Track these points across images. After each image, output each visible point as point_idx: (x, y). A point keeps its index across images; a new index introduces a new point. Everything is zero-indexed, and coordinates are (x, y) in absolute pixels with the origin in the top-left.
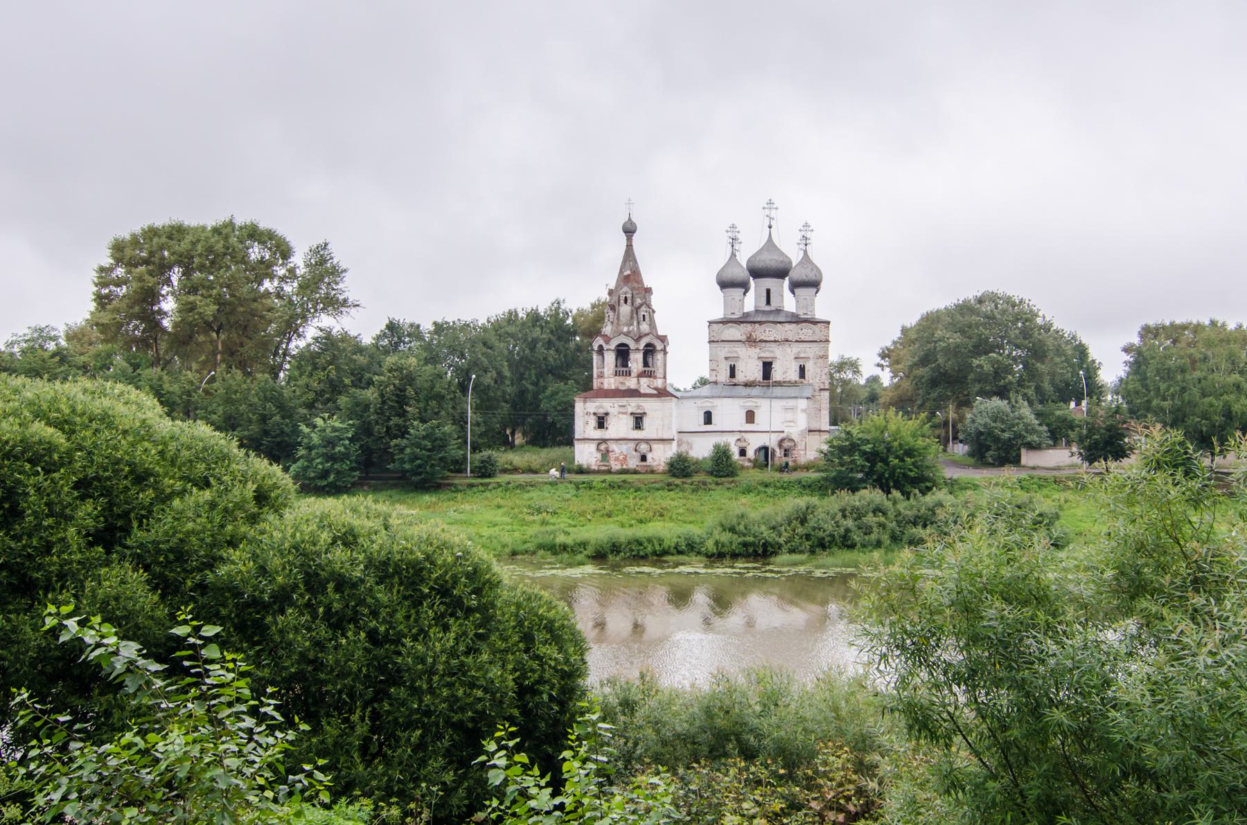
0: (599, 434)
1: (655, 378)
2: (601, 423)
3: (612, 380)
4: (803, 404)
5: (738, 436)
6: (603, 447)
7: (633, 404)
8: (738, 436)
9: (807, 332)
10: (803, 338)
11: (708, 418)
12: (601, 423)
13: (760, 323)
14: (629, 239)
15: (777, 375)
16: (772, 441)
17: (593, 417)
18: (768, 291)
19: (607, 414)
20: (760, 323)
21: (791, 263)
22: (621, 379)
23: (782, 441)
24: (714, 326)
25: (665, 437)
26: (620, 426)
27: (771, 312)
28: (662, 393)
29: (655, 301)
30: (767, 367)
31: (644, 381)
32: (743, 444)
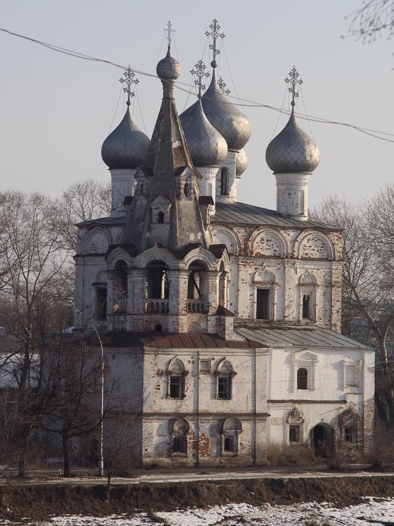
0: (170, 406)
2: (176, 389)
5: (290, 407)
8: (290, 407)
12: (176, 389)
16: (328, 415)
22: (195, 317)
30: (263, 297)
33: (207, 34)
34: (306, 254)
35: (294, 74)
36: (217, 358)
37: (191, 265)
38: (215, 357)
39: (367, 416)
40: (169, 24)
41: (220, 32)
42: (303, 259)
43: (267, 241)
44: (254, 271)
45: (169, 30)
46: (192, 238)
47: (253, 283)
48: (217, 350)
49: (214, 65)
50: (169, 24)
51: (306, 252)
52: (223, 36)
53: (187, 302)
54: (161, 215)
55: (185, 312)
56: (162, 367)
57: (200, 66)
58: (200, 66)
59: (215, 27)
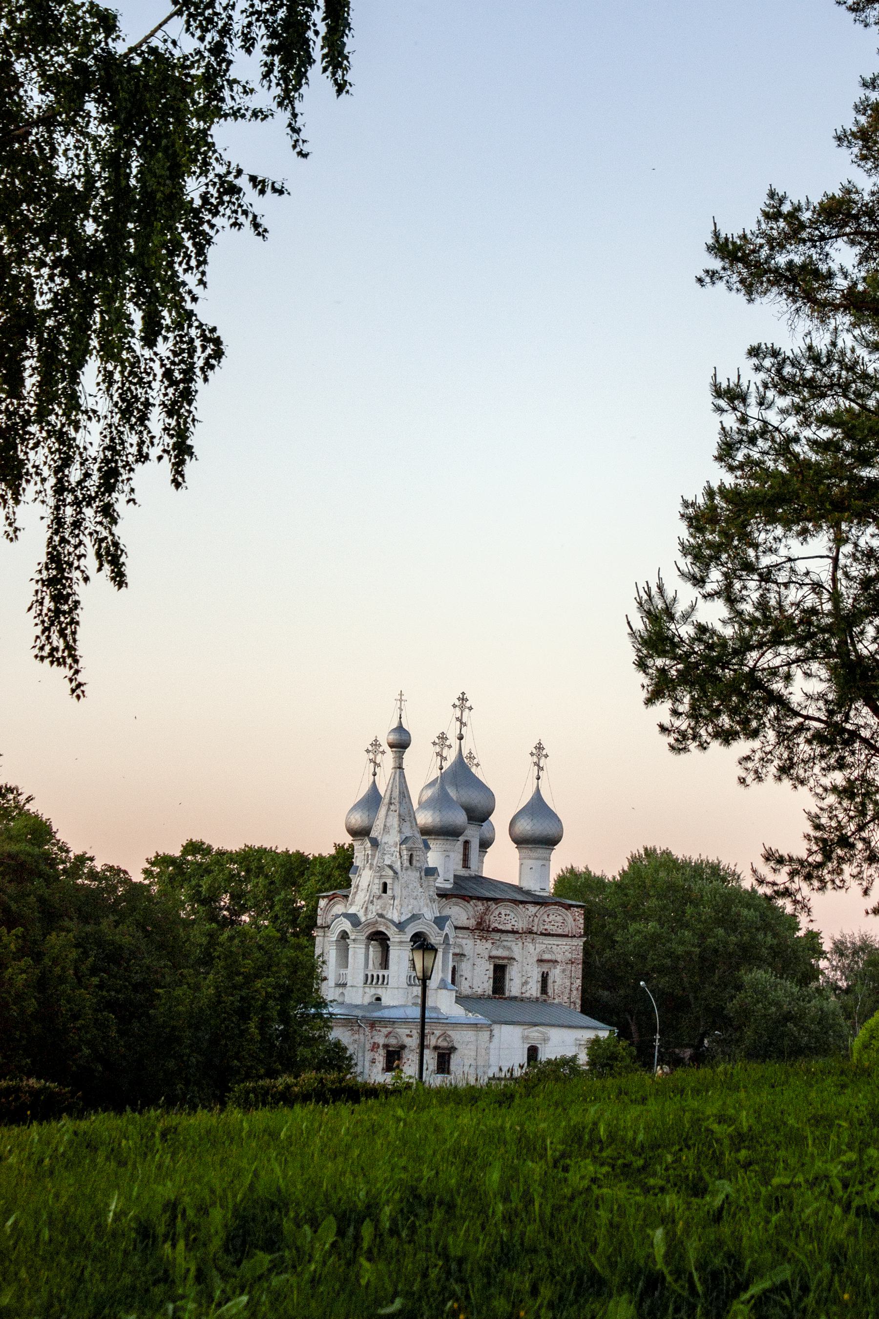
14: (399, 759)
15: (514, 987)
18: (466, 843)
19: (403, 1047)
20: (496, 900)
30: (500, 971)
33: (454, 706)
35: (539, 747)
36: (438, 1033)
40: (401, 695)
41: (468, 704)
45: (401, 700)
49: (461, 738)
50: (401, 695)
52: (470, 709)
54: (385, 885)
56: (381, 1041)
57: (443, 737)
58: (443, 737)
59: (463, 699)
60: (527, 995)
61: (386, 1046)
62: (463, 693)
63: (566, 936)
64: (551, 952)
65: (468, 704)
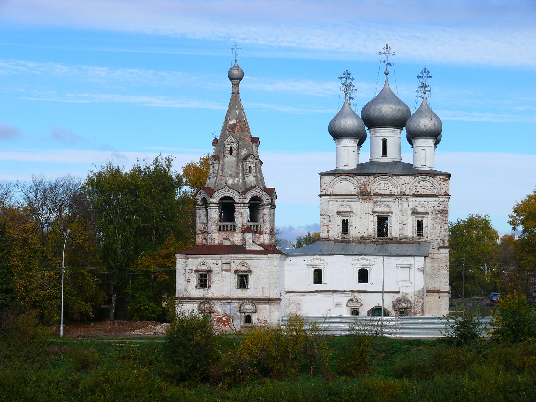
0: (200, 293)
1: (261, 233)
2: (204, 280)
3: (216, 236)
4: (419, 261)
5: (350, 296)
6: (205, 307)
7: (237, 262)
8: (350, 296)
9: (425, 185)
10: (421, 191)
11: (318, 277)
12: (204, 280)
13: (375, 175)
15: (394, 231)
17: (195, 275)
18: (384, 142)
19: (210, 271)
21: (409, 111)
23: (398, 301)
24: (327, 179)
25: (272, 297)
26: (223, 285)
27: (387, 164)
28: (269, 250)
29: (263, 153)
30: (382, 223)
31: (249, 236)
32: (356, 305)
34: (418, 192)
36: (237, 262)
37: (250, 200)
38: (235, 261)
39: (418, 302)
42: (414, 195)
43: (384, 184)
44: (373, 205)
46: (230, 182)
47: (374, 212)
48: (236, 255)
51: (418, 190)
53: (219, 224)
55: (216, 231)
60: (405, 235)
61: (197, 271)
62: (387, 45)
63: (435, 195)
64: (423, 207)
65: (392, 51)
